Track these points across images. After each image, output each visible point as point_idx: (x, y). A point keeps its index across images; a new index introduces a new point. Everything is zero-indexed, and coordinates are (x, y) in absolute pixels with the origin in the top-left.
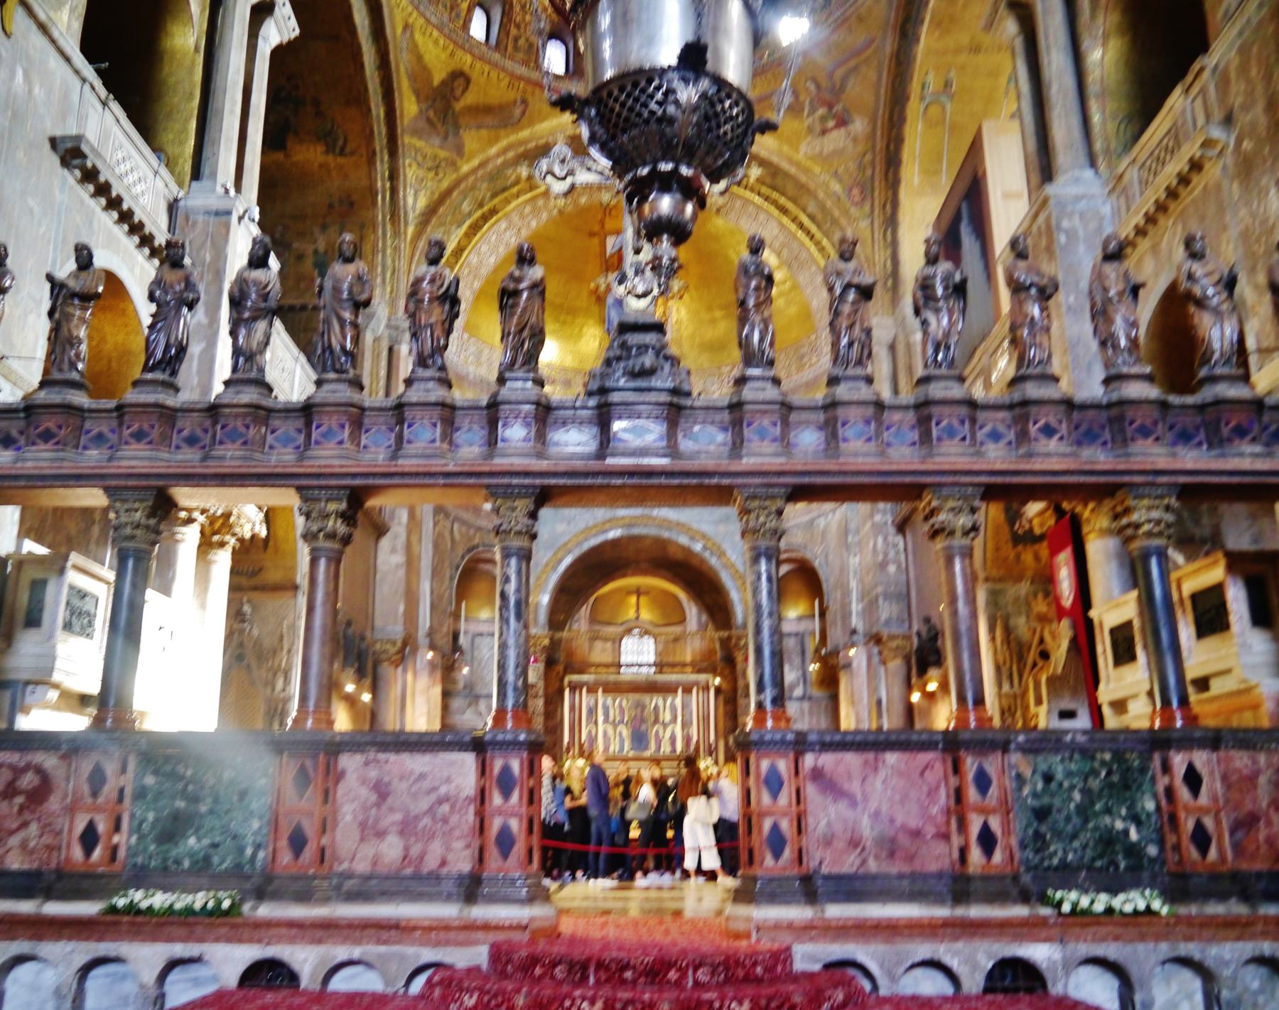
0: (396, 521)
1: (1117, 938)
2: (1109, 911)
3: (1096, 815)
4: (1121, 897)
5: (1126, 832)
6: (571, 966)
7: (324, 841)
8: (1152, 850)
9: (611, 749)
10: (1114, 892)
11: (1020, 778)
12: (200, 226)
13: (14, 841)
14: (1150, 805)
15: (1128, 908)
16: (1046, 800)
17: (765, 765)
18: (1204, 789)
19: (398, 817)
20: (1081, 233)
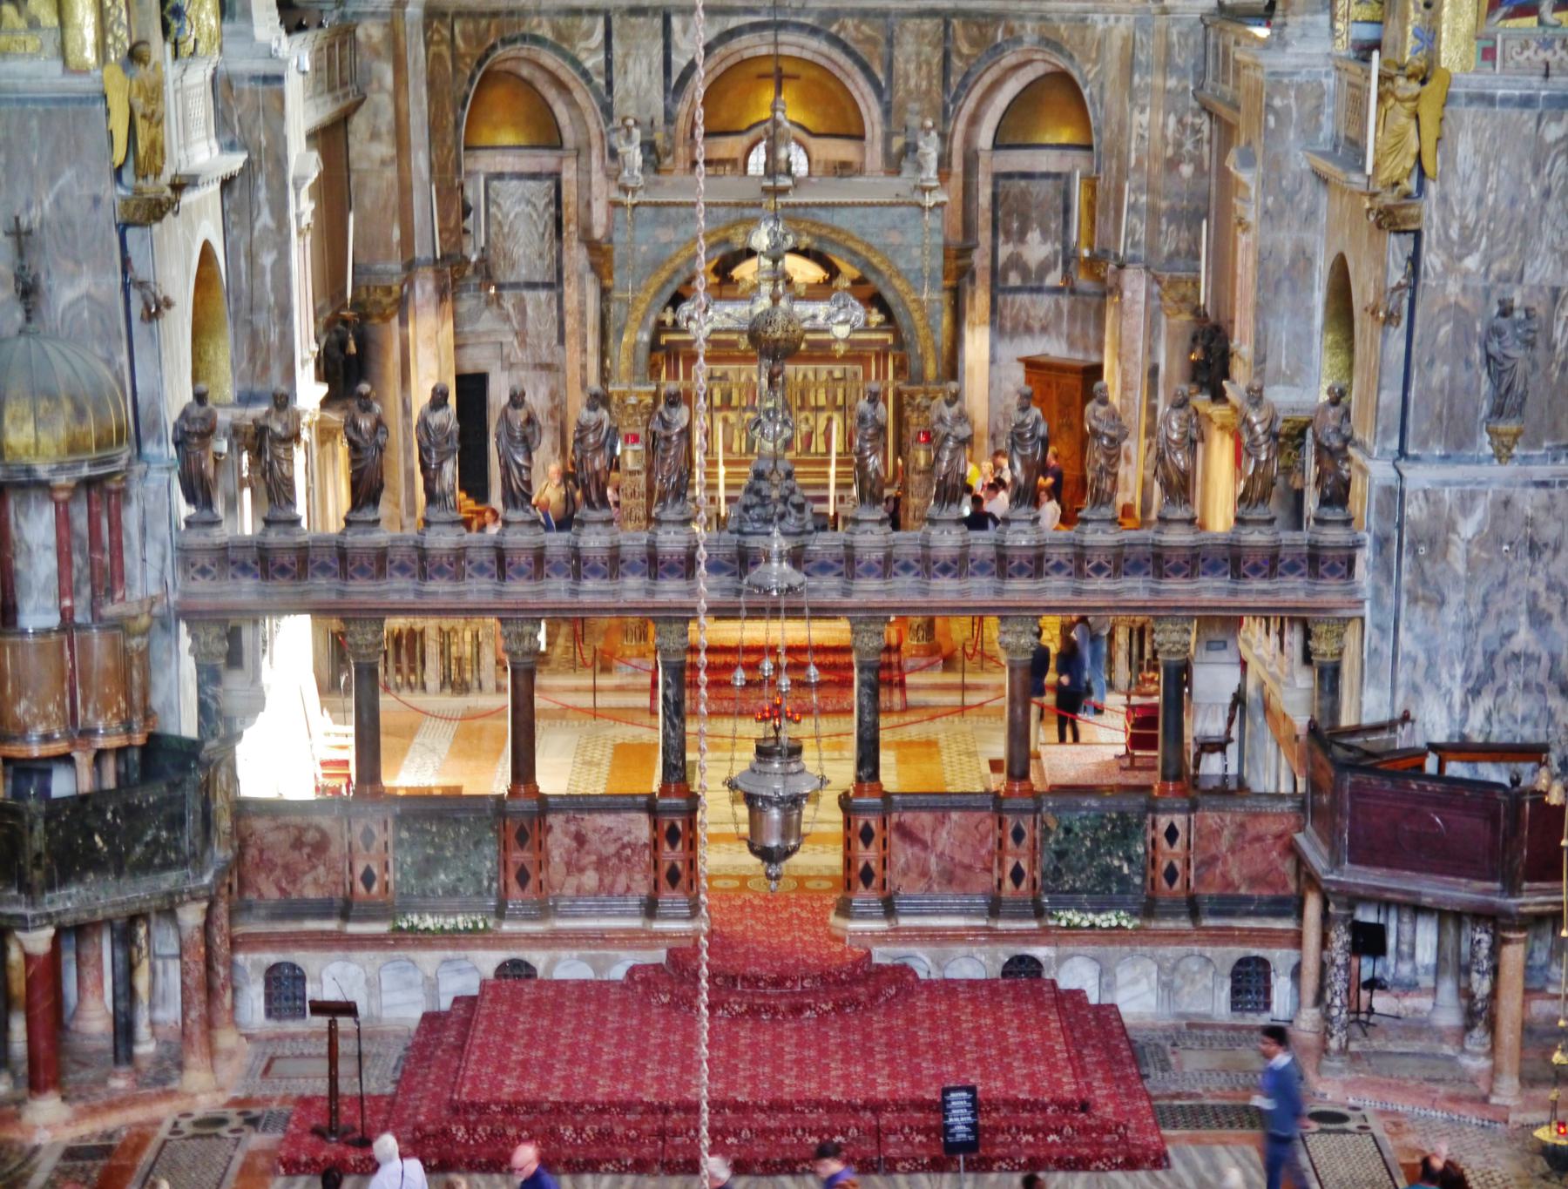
0: (375, 85)
1: (1094, 944)
2: (1092, 926)
3: (1100, 856)
4: (1103, 916)
5: (1120, 868)
6: (726, 977)
7: (542, 876)
8: (1138, 880)
9: (735, 447)
10: (1098, 912)
11: (1047, 831)
12: (247, 98)
13: (308, 878)
14: (1140, 850)
15: (1105, 925)
16: (1065, 845)
17: (861, 823)
18: (1178, 841)
19: (594, 858)
20: (1295, 115)
